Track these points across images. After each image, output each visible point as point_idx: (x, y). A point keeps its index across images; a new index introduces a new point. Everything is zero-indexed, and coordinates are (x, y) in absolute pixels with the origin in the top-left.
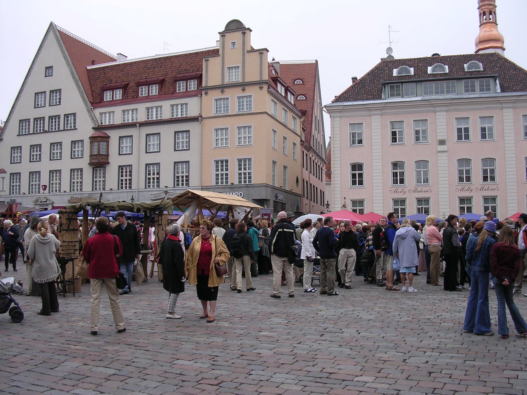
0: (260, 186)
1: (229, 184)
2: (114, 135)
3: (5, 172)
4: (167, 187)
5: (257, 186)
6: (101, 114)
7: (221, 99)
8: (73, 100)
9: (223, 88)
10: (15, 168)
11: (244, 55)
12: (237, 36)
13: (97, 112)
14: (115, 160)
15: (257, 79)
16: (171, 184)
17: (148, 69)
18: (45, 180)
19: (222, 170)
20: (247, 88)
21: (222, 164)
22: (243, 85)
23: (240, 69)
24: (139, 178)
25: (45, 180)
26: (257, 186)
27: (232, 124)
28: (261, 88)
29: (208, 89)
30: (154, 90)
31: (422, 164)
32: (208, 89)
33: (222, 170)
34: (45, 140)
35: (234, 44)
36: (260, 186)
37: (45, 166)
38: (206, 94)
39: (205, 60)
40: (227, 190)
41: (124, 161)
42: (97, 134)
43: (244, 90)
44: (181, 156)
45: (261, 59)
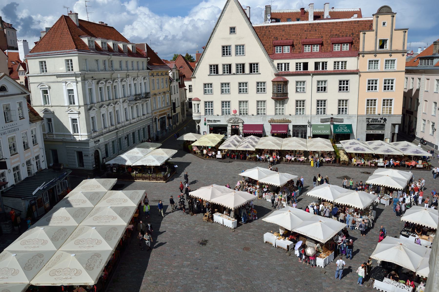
1: (376, 113)
2: (292, 80)
3: (200, 101)
4: (332, 115)
6: (278, 64)
8: (255, 52)
10: (208, 98)
12: (387, 18)
13: (276, 62)
14: (293, 95)
15: (400, 48)
16: (335, 112)
17: (305, 31)
18: (234, 106)
19: (371, 105)
21: (371, 102)
22: (391, 53)
24: (310, 108)
25: (234, 106)
28: (403, 55)
29: (364, 53)
30: (316, 49)
34: (234, 80)
35: (384, 24)
37: (234, 97)
38: (363, 56)
41: (300, 97)
42: (280, 79)
44: (343, 96)
45: (404, 36)
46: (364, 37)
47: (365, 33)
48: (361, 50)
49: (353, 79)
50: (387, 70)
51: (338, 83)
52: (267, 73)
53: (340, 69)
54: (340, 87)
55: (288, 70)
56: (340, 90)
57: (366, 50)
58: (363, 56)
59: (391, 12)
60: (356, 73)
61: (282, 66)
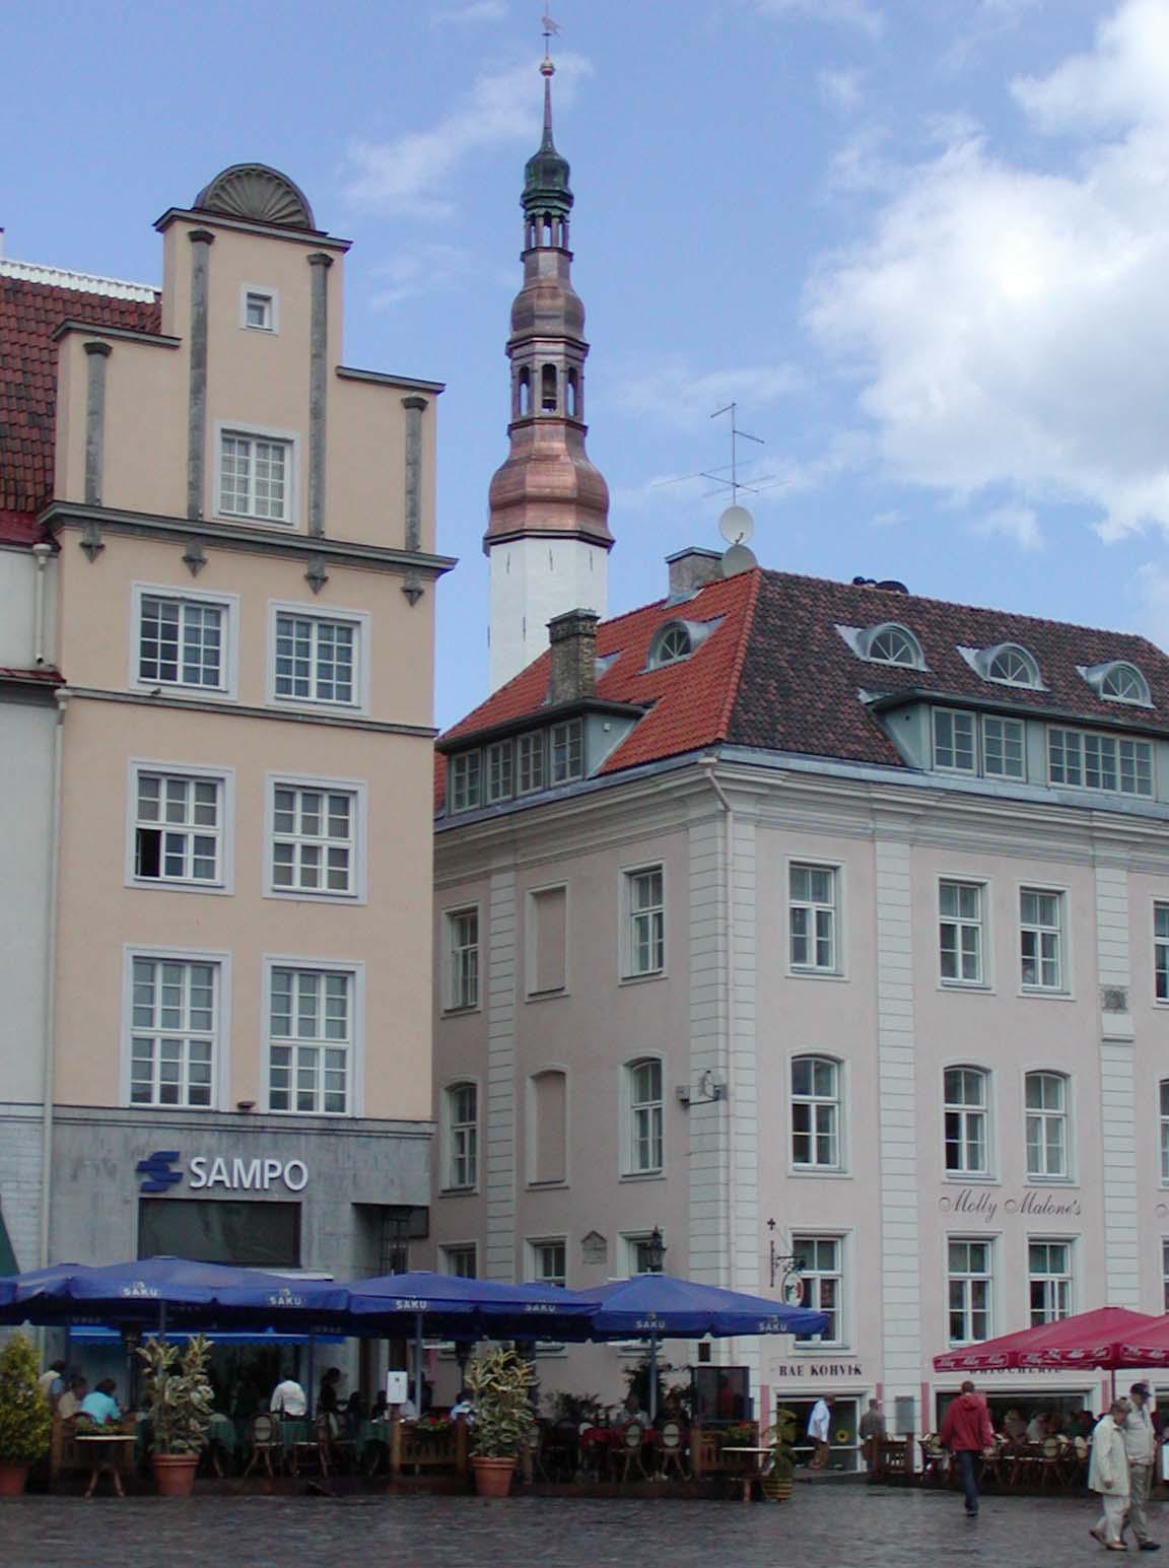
0: (401, 1136)
5: (386, 1135)
7: (171, 605)
9: (196, 537)
11: (319, 386)
20: (334, 573)
23: (296, 462)
26: (386, 1135)
27: (250, 765)
29: (103, 524)
31: (1042, 1085)
32: (103, 524)
33: (173, 1018)
36: (401, 1136)
38: (92, 549)
39: (91, 349)
40: (209, 1140)
43: (316, 581)
46: (97, 385)
47: (103, 351)
48: (70, 488)
50: (294, 704)
57: (116, 496)
58: (92, 549)
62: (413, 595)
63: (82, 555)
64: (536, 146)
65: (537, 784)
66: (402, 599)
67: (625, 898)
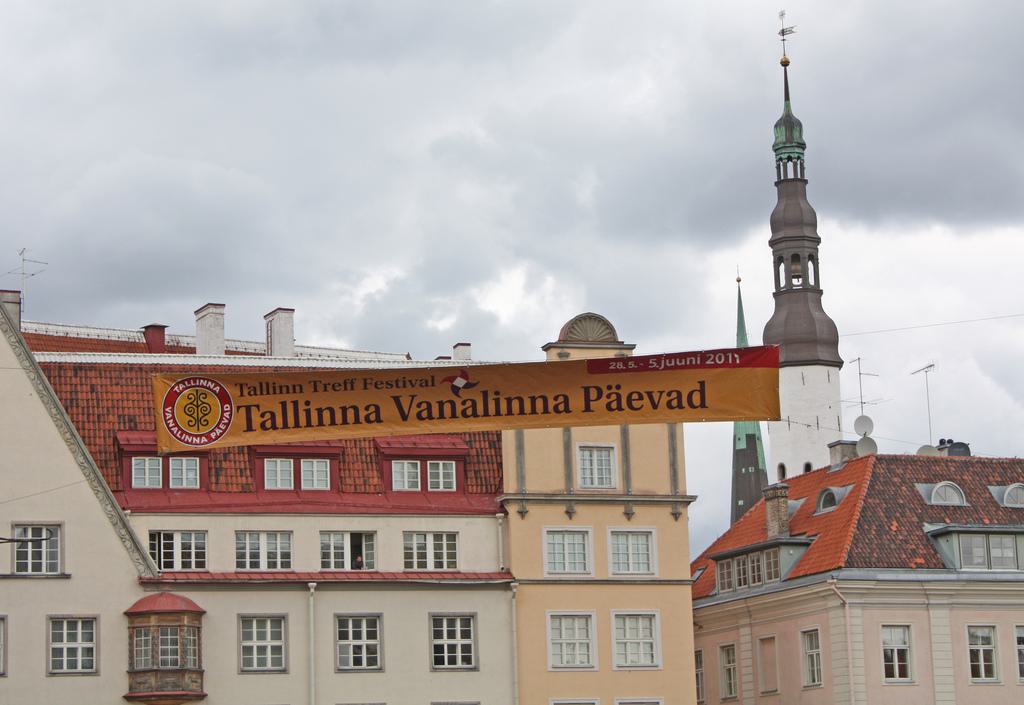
2: (221, 611)
6: (153, 536)
13: (143, 525)
20: (636, 509)
23: (616, 457)
29: (525, 500)
32: (525, 500)
38: (522, 514)
48: (510, 486)
49: (488, 608)
51: (425, 629)
52: (103, 572)
53: (431, 567)
54: (438, 649)
55: (201, 564)
56: (439, 661)
57: (533, 486)
58: (522, 514)
59: (616, 341)
60: (502, 581)
61: (170, 546)
62: (676, 516)
63: (518, 517)
64: (780, 113)
65: (759, 581)
66: (671, 518)
67: (802, 646)
